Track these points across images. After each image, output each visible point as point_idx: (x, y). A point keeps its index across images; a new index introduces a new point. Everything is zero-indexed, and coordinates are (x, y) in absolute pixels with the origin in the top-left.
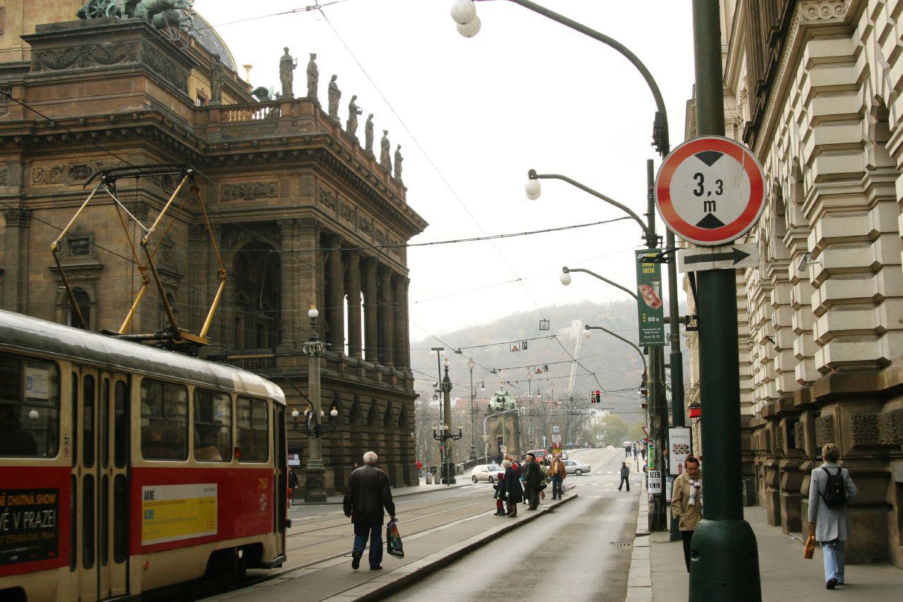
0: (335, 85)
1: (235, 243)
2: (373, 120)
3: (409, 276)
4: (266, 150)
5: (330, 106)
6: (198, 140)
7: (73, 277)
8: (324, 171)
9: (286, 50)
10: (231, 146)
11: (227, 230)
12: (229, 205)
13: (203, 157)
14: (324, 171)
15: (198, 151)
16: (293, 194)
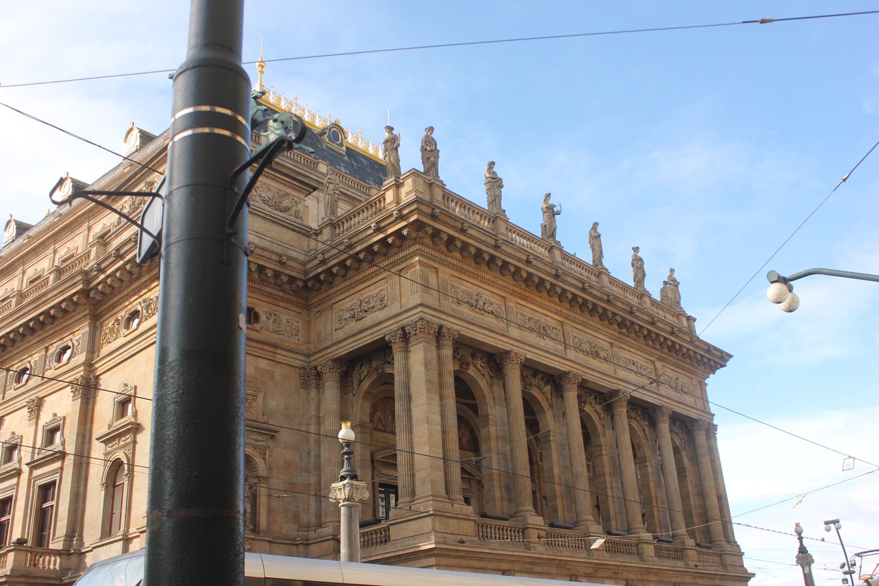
0: (494, 173)
1: (361, 382)
2: (599, 230)
3: (715, 422)
4: (358, 248)
5: (635, 276)
6: (281, 256)
7: (116, 446)
8: (455, 262)
9: (390, 129)
10: (327, 256)
11: (348, 365)
12: (341, 334)
13: (305, 282)
14: (455, 262)
15: (287, 272)
16: (399, 296)
